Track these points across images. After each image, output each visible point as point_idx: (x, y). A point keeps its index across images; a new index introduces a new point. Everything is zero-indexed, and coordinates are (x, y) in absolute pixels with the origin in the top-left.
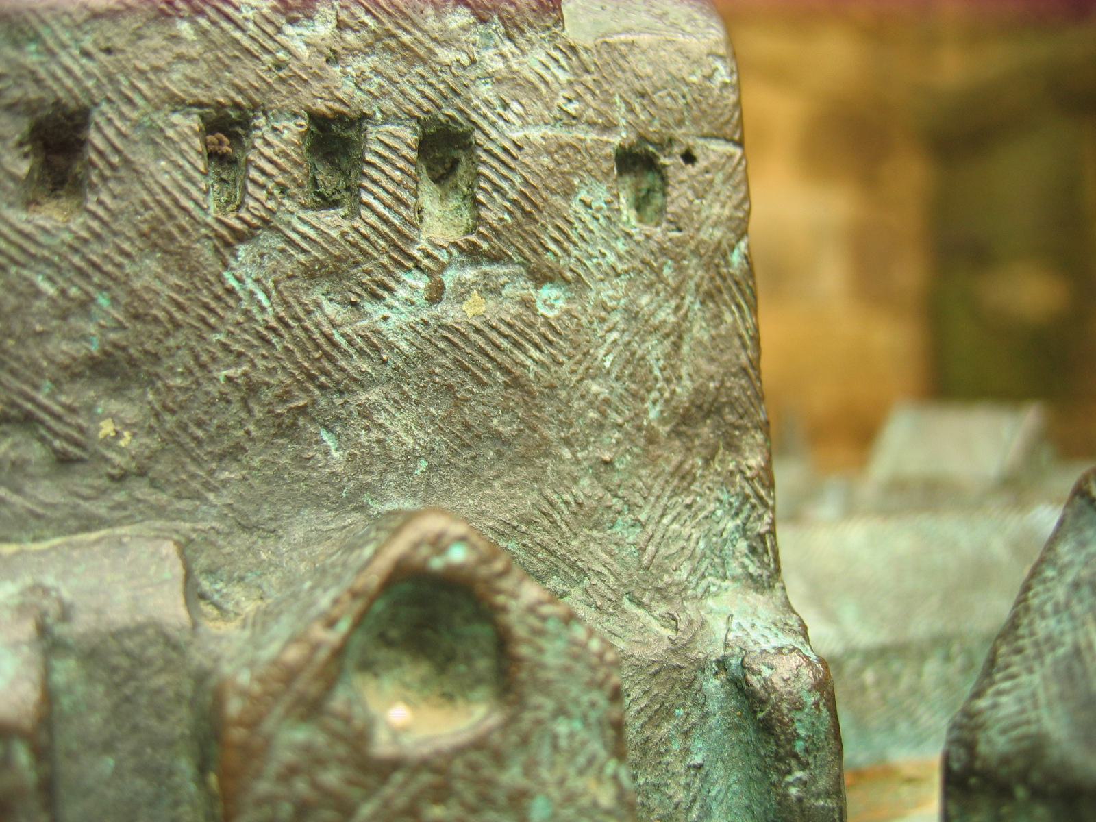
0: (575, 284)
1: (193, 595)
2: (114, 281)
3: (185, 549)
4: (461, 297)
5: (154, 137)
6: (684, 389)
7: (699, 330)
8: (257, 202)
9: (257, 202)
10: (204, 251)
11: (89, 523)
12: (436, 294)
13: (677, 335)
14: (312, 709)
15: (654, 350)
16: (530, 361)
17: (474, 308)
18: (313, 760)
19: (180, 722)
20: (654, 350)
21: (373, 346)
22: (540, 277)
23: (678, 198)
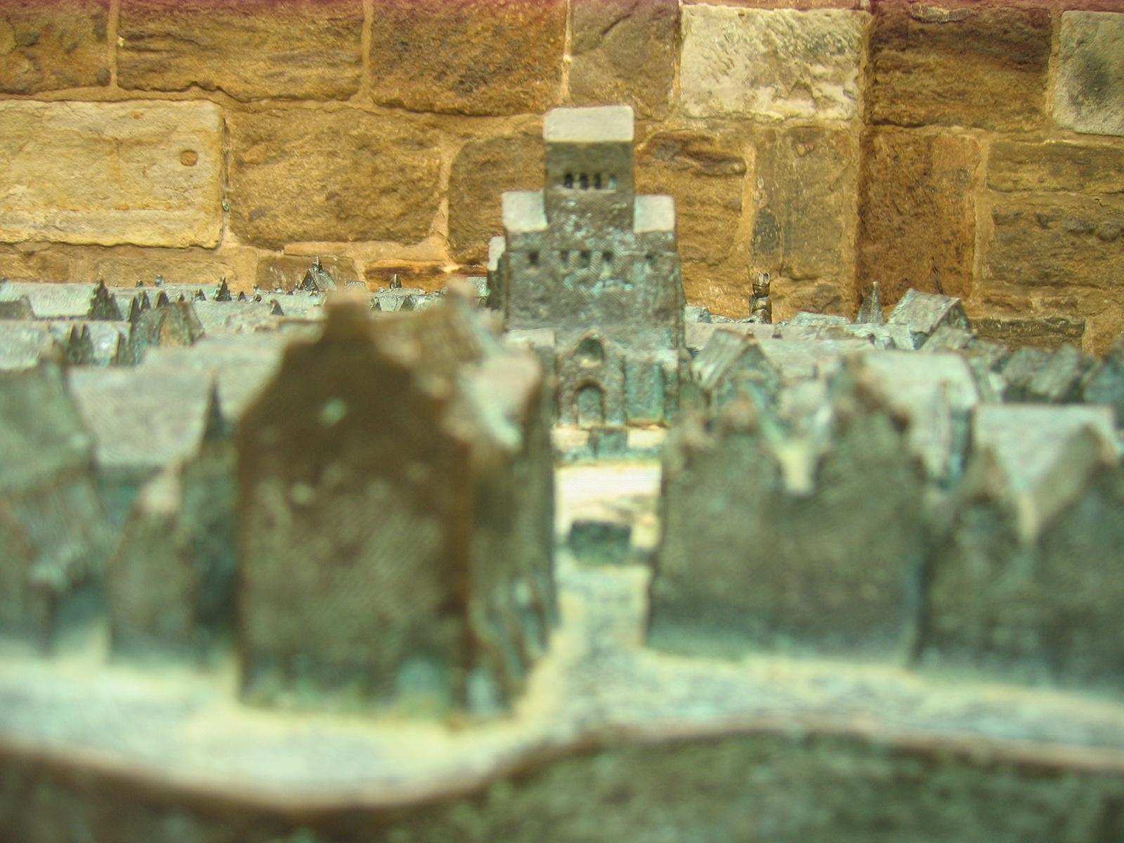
0: (634, 284)
1: (556, 342)
2: (543, 283)
3: (555, 334)
4: (610, 286)
5: (551, 256)
6: (657, 306)
7: (662, 294)
8: (571, 268)
9: (571, 268)
10: (560, 278)
11: (537, 328)
12: (604, 286)
13: (656, 295)
14: (571, 358)
15: (651, 299)
16: (623, 299)
17: (612, 289)
18: (570, 367)
19: (552, 363)
20: (651, 299)
21: (591, 296)
22: (627, 282)
23: (659, 265)
